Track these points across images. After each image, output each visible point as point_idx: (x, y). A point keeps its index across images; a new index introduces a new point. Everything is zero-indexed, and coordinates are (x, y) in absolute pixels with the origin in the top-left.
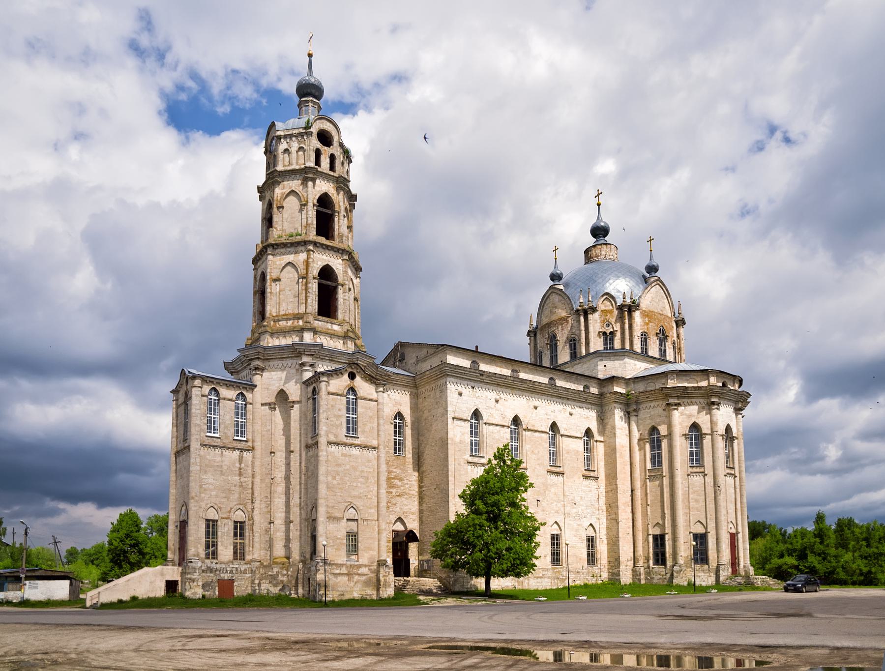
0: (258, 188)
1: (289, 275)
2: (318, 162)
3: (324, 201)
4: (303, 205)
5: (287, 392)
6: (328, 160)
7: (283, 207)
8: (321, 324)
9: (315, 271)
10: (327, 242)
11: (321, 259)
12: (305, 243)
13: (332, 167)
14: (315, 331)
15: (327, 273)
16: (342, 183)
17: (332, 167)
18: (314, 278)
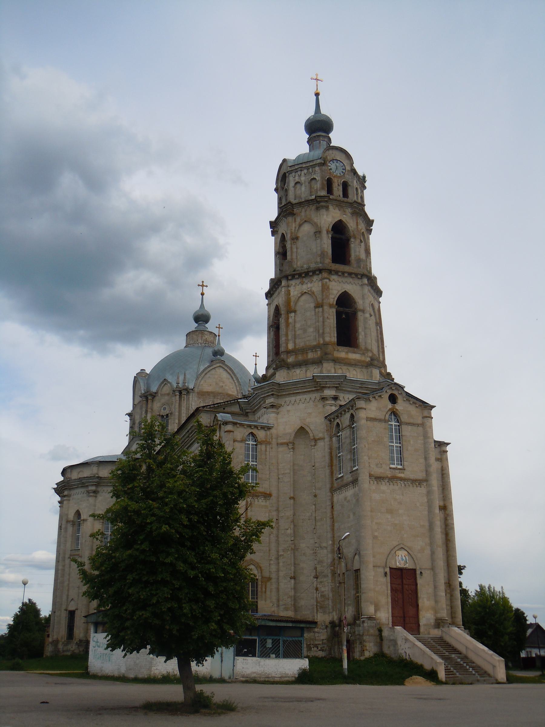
0: (271, 223)
1: (306, 305)
2: (330, 190)
3: (339, 229)
4: (318, 233)
5: (307, 429)
6: (341, 188)
7: (297, 238)
8: (342, 353)
9: (333, 298)
10: (346, 268)
11: (337, 286)
12: (320, 271)
13: (345, 194)
14: (336, 361)
15: (345, 301)
16: (358, 209)
17: (345, 194)
18: (331, 306)
